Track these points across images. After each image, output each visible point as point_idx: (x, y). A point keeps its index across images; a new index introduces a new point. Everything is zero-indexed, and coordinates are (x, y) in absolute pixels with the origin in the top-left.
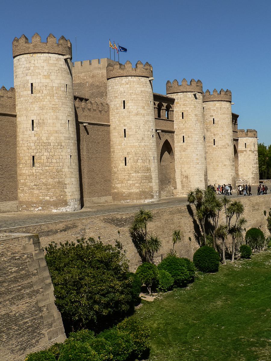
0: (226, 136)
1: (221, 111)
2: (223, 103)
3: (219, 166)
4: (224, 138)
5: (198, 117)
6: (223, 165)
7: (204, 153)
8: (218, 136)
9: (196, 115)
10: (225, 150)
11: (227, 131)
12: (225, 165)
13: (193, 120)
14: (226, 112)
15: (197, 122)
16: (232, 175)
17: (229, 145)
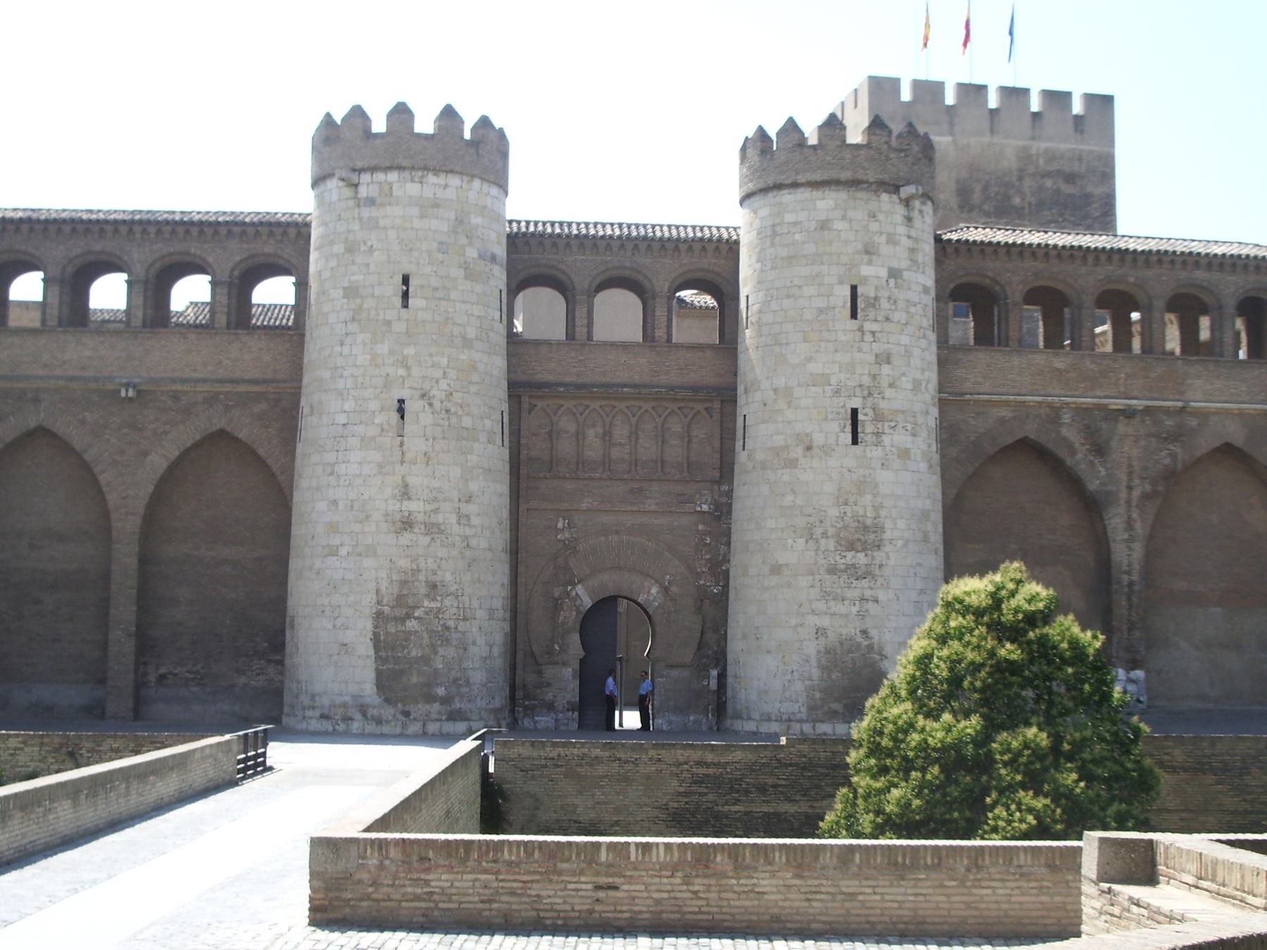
0: (799, 392)
1: (773, 245)
2: (787, 197)
3: (753, 571)
4: (782, 404)
5: (358, 301)
6: (766, 569)
7: (388, 492)
8: (758, 396)
9: (351, 292)
10: (786, 478)
11: (809, 359)
12: (776, 569)
13: (332, 318)
14: (810, 248)
15: (353, 327)
16: (820, 632)
17: (815, 444)
